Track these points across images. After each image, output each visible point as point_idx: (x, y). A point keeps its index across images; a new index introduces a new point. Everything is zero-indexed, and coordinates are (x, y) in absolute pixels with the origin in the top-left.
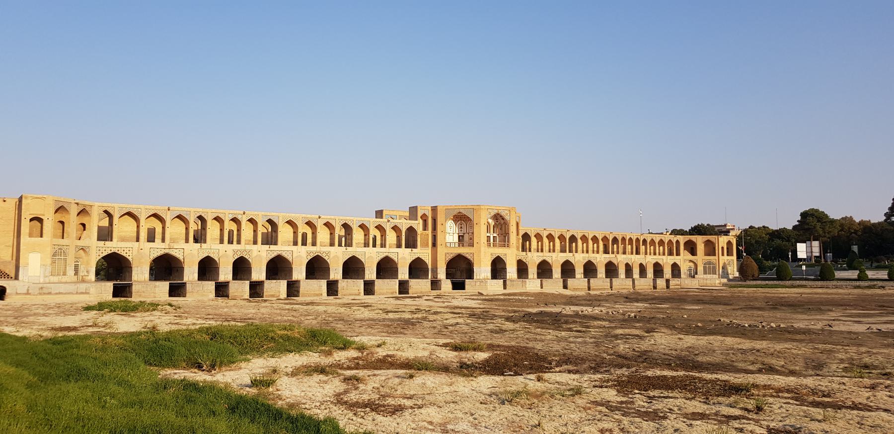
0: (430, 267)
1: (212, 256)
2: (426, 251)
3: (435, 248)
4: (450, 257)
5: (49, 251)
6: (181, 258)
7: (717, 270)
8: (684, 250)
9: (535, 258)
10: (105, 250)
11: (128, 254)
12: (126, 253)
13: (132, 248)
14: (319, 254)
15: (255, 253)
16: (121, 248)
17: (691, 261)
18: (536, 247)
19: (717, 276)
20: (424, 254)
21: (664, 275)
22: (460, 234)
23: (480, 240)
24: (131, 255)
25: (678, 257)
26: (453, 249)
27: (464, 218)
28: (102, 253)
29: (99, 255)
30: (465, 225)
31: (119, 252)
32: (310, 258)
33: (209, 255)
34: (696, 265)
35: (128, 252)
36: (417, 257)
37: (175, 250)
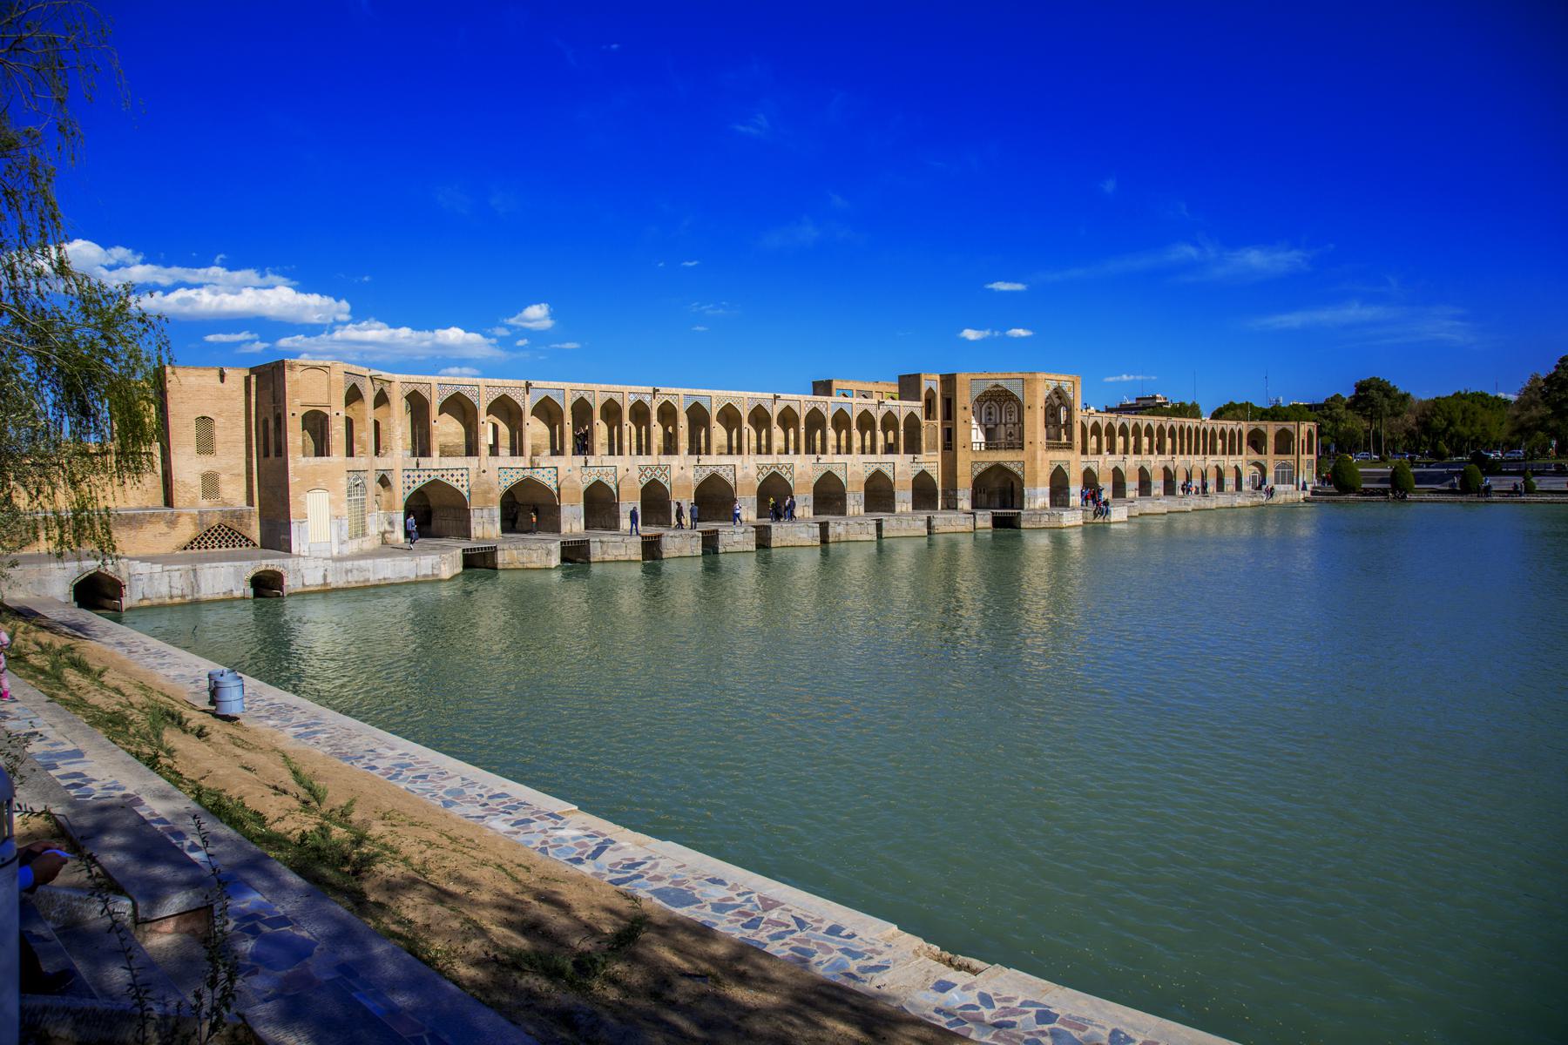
0: (940, 488)
2: (933, 459)
3: (952, 453)
4: (980, 470)
5: (343, 482)
6: (553, 487)
7: (1295, 477)
8: (1248, 444)
9: (492, 475)
10: (419, 476)
11: (460, 483)
12: (457, 481)
13: (467, 469)
14: (776, 470)
15: (675, 473)
17: (1256, 464)
19: (1295, 487)
20: (933, 464)
21: (1225, 487)
22: (988, 426)
23: (1035, 437)
24: (465, 483)
25: (1240, 457)
26: (984, 454)
27: (999, 395)
28: (414, 482)
29: (409, 488)
30: (998, 408)
31: (444, 480)
32: (762, 478)
35: (460, 478)
36: (921, 469)
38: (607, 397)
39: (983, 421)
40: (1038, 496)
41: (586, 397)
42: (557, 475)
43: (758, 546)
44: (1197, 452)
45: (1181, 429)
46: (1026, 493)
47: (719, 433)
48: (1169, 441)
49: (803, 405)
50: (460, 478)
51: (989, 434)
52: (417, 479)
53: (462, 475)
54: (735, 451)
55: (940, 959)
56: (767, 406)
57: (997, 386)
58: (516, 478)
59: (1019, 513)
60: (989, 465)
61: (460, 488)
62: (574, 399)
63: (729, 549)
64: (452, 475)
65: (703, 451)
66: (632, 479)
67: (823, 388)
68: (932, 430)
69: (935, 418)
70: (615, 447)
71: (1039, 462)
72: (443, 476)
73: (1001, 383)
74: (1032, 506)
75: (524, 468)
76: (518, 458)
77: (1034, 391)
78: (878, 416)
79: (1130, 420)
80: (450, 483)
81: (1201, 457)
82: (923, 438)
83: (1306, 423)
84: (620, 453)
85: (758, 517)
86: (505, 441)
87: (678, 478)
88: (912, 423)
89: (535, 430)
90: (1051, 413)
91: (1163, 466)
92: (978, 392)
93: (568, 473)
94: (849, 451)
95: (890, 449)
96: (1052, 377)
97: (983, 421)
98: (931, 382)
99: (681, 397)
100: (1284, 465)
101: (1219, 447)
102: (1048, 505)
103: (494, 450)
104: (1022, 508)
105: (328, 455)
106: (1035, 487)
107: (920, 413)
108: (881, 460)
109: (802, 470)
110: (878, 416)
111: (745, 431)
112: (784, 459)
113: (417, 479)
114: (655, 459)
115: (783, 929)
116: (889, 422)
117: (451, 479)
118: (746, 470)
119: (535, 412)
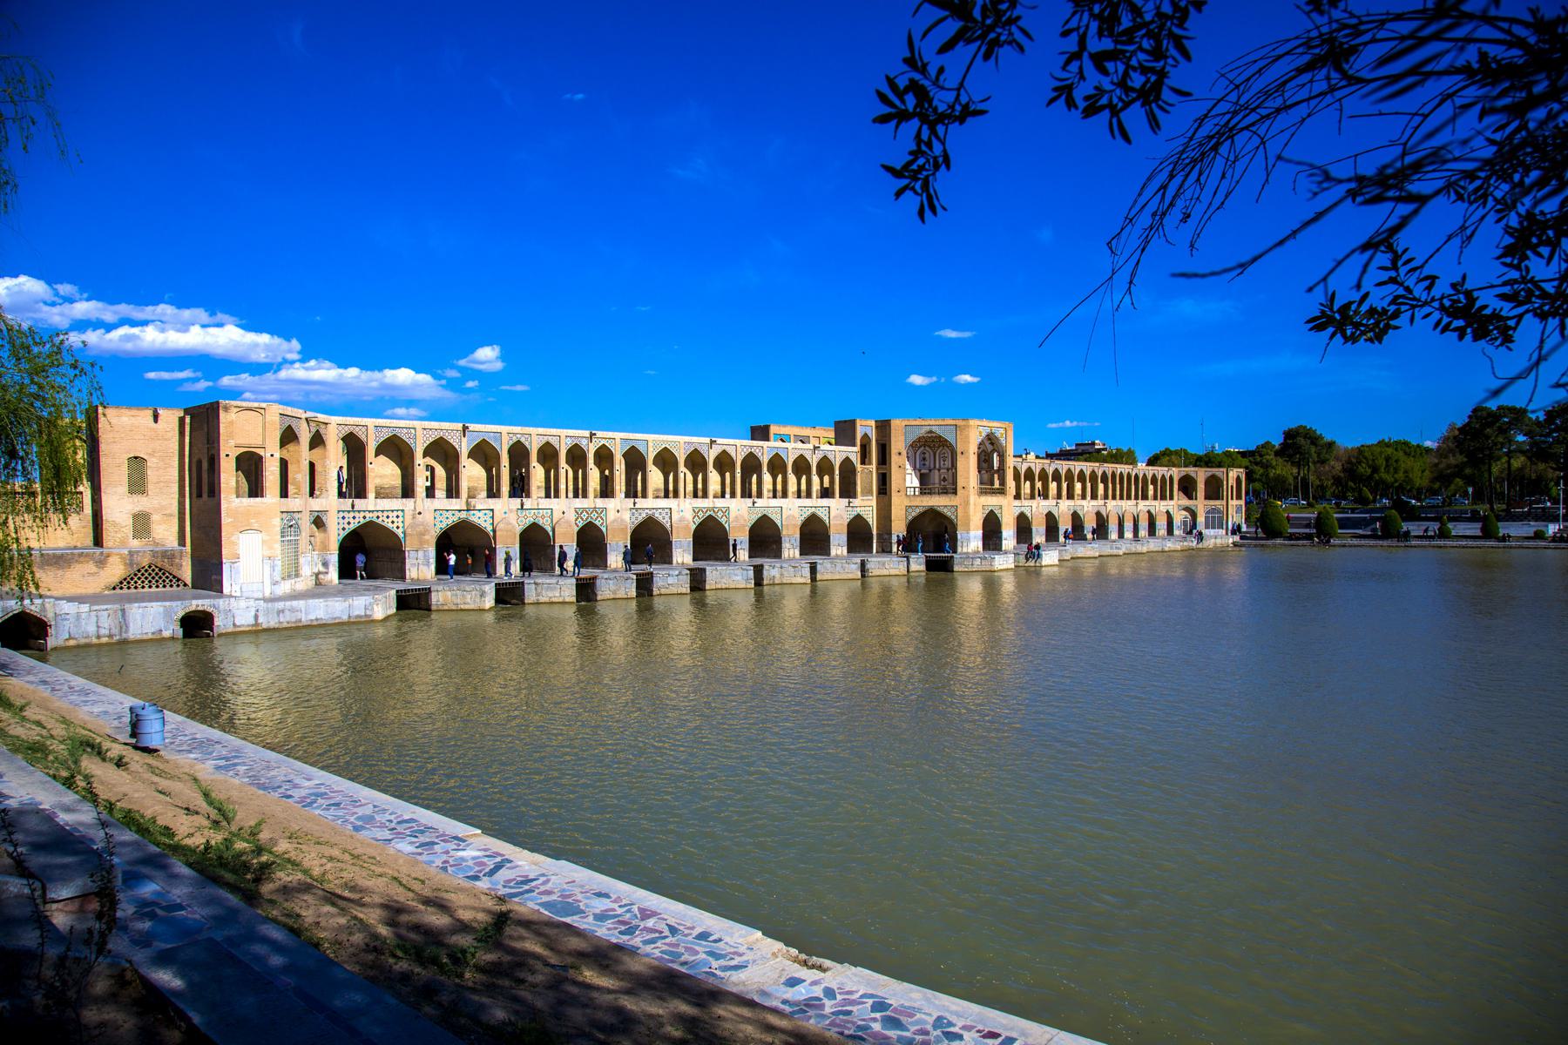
0: (875, 532)
1: (540, 523)
4: (914, 514)
5: (277, 523)
6: (489, 529)
9: (428, 517)
10: (354, 518)
11: (395, 525)
12: (393, 522)
13: (403, 511)
14: (712, 513)
15: (612, 516)
16: (383, 511)
17: (1187, 509)
18: (795, 488)
19: (1224, 532)
23: (968, 482)
24: (401, 525)
25: (1172, 503)
26: (919, 499)
28: (349, 523)
29: (344, 529)
31: (379, 521)
32: (698, 521)
33: (536, 521)
34: (1194, 515)
35: (395, 520)
37: (481, 514)
38: (544, 440)
39: (918, 466)
40: (971, 540)
41: (523, 440)
42: (493, 517)
43: (692, 589)
44: (1129, 498)
45: (1114, 475)
46: (959, 537)
47: (655, 477)
48: (1101, 486)
49: (739, 449)
50: (395, 520)
51: (923, 479)
52: (352, 521)
53: (398, 517)
54: (671, 495)
55: (795, 960)
56: (704, 450)
57: (931, 432)
58: (451, 520)
59: (952, 557)
60: (922, 510)
61: (395, 530)
62: (511, 443)
63: (663, 591)
64: (388, 517)
65: (640, 494)
66: (568, 522)
67: (761, 433)
68: (867, 475)
69: (870, 463)
70: (551, 491)
71: (972, 507)
72: (378, 517)
73: (934, 429)
74: (965, 550)
75: (460, 511)
76: (454, 500)
77: (967, 437)
78: (814, 461)
79: (1063, 466)
80: (384, 524)
81: (1133, 502)
82: (859, 482)
83: (1235, 470)
84: (557, 496)
85: (694, 560)
86: (441, 484)
87: (614, 521)
88: (848, 468)
89: (473, 472)
90: (984, 460)
91: (1046, 511)
92: (913, 437)
93: (504, 516)
94: (785, 495)
95: (826, 493)
96: (985, 423)
97: (918, 466)
98: (866, 427)
99: (618, 441)
100: (1213, 511)
101: (1151, 492)
102: (981, 549)
103: (430, 492)
104: (955, 552)
105: (262, 496)
106: (968, 530)
107: (855, 459)
108: (816, 505)
109: (738, 514)
110: (814, 461)
111: (682, 475)
112: (720, 503)
113: (352, 521)
114: (592, 501)
115: (657, 935)
116: (825, 467)
117: (386, 520)
118: (682, 514)
119: (471, 455)
